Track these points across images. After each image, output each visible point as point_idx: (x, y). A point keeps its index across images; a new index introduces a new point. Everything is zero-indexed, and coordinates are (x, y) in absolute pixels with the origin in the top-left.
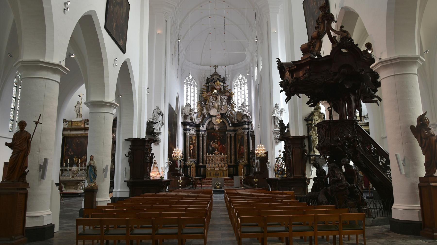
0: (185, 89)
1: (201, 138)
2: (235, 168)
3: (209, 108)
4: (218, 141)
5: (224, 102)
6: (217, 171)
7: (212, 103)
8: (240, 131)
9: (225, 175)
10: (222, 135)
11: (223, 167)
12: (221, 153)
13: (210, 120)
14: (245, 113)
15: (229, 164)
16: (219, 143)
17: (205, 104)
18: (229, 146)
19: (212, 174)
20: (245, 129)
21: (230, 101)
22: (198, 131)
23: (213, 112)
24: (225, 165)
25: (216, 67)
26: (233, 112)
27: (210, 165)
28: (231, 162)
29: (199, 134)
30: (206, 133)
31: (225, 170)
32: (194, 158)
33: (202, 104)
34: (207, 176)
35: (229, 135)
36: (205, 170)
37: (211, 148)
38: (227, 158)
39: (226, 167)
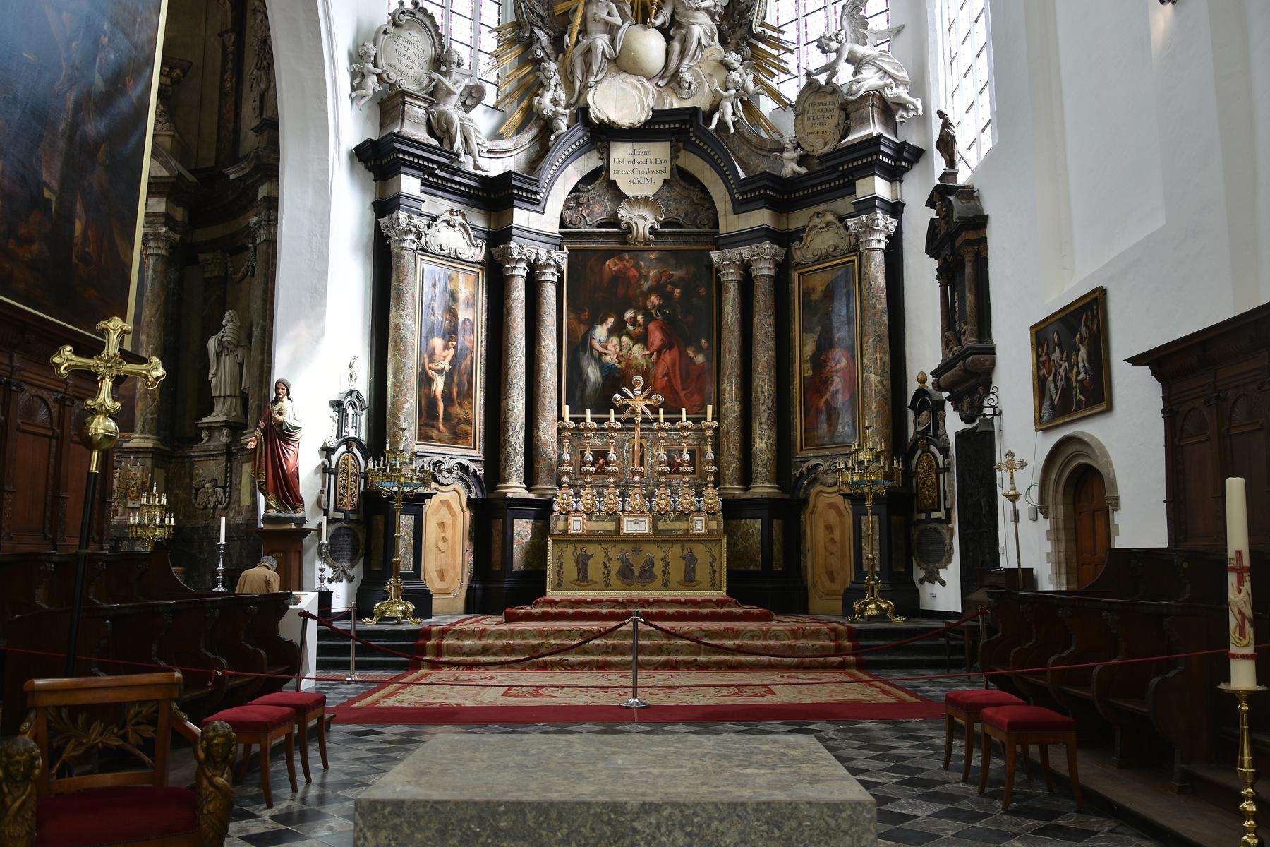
1: (518, 292)
2: (776, 525)
3: (587, 70)
4: (649, 318)
7: (611, 30)
8: (822, 241)
9: (702, 572)
10: (677, 274)
11: (684, 516)
12: (672, 410)
13: (589, 162)
14: (871, 79)
15: (735, 490)
16: (656, 337)
17: (558, 44)
18: (731, 357)
19: (595, 570)
20: (869, 205)
22: (498, 237)
23: (619, 101)
24: (699, 495)
26: (767, 106)
27: (587, 493)
28: (746, 477)
29: (507, 256)
30: (562, 258)
31: (699, 540)
32: (458, 436)
33: (532, 40)
34: (559, 585)
35: (731, 276)
36: (542, 531)
37: (593, 373)
38: (717, 448)
39: (711, 515)
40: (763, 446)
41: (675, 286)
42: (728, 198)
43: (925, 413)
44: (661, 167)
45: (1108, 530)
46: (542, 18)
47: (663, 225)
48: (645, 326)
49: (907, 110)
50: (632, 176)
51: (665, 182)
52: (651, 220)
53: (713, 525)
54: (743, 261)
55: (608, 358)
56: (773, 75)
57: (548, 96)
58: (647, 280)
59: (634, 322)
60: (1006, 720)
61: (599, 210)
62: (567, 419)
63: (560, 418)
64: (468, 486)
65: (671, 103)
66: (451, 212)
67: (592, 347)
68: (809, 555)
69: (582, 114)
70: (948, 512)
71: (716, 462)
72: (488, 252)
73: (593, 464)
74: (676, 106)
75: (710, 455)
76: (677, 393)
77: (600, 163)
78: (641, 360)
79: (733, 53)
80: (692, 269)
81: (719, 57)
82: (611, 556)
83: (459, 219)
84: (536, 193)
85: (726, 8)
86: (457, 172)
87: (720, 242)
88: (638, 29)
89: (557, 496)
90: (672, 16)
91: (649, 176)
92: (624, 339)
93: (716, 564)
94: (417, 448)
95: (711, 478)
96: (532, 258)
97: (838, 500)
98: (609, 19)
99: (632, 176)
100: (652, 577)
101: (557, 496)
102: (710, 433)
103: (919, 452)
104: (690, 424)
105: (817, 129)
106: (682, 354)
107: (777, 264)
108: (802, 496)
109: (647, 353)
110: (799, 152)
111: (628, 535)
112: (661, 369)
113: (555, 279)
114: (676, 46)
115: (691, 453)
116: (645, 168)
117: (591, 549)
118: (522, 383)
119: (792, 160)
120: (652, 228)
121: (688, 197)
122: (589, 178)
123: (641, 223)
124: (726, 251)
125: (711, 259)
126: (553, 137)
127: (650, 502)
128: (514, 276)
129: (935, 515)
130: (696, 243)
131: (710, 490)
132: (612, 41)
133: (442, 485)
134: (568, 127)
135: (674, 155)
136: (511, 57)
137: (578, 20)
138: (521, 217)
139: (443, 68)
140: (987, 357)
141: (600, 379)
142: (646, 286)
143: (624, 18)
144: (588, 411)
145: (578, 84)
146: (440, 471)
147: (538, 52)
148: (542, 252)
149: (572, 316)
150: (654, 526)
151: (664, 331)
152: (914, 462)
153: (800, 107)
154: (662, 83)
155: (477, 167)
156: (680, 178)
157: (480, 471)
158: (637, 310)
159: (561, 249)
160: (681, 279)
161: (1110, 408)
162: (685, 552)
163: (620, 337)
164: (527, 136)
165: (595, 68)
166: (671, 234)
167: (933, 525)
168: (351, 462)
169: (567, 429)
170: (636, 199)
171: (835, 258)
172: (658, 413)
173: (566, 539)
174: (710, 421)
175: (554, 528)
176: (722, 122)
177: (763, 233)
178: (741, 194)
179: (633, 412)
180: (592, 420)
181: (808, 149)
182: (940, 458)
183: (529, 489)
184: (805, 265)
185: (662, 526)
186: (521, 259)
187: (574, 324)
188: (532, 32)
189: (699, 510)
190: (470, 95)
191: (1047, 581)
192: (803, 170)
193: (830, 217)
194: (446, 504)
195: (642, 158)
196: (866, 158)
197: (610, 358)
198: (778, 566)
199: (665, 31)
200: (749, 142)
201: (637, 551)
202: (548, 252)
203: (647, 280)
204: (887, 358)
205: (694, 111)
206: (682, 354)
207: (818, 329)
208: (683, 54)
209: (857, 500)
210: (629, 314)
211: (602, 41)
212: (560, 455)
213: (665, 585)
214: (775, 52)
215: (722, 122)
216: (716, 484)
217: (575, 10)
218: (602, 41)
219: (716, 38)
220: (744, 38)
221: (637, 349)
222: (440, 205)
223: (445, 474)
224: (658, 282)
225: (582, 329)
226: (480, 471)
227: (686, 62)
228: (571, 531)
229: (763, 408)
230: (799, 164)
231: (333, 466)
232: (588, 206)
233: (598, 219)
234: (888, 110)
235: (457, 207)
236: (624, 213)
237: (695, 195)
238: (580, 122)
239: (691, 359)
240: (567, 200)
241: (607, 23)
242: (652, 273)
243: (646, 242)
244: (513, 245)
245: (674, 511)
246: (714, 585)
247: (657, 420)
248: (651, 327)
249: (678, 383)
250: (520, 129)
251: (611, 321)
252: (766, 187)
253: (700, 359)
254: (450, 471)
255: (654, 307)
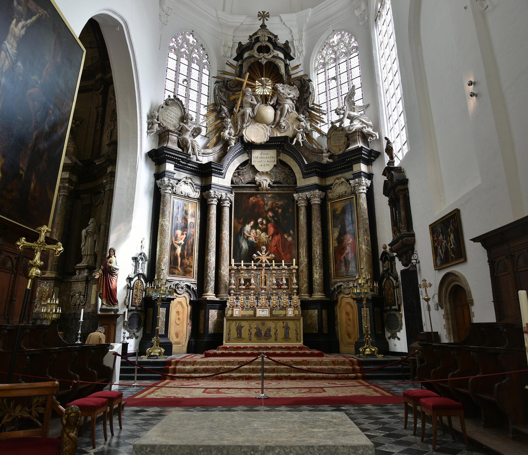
0: (172, 64)
1: (213, 211)
3: (243, 122)
4: (268, 221)
5: (288, 105)
6: (263, 319)
7: (253, 106)
8: (340, 189)
9: (292, 334)
10: (280, 203)
11: (284, 308)
12: (278, 261)
13: (244, 158)
15: (306, 296)
16: (271, 230)
17: (231, 112)
18: (303, 238)
19: (245, 333)
21: (304, 103)
22: (205, 188)
23: (255, 134)
24: (290, 298)
25: (264, 16)
26: (316, 135)
29: (209, 196)
30: (232, 197)
32: (186, 273)
35: (302, 204)
36: (222, 315)
37: (244, 245)
38: (298, 278)
39: (296, 307)
40: (318, 277)
41: (279, 208)
42: (300, 172)
43: (387, 262)
44: (273, 160)
45: (469, 315)
46: (225, 102)
47: (273, 184)
48: (267, 225)
49: (372, 137)
50: (261, 163)
51: (275, 166)
52: (269, 181)
53: (297, 312)
54: (307, 198)
55: (251, 239)
56: (318, 123)
57: (227, 132)
58: (267, 206)
59: (262, 223)
60: (431, 404)
61: (247, 177)
62: (233, 265)
63: (230, 265)
64: (190, 295)
65: (277, 134)
66: (186, 178)
67: (244, 234)
68: (339, 326)
69: (240, 139)
70: (399, 306)
71: (297, 284)
72: (201, 194)
73: (244, 285)
74: (279, 135)
75: (295, 281)
76: (280, 254)
77: (248, 158)
78: (265, 239)
79: (302, 115)
80: (286, 201)
81: (296, 116)
82: (252, 326)
83: (190, 181)
84: (222, 170)
85: (298, 98)
86: (190, 162)
87: (297, 190)
88: (263, 106)
89: (228, 299)
90: (277, 101)
91: (268, 163)
92: (258, 230)
93: (298, 330)
94: (168, 278)
95: (295, 291)
96: (219, 197)
97: (351, 301)
98: (252, 102)
99: (261, 163)
100: (270, 336)
101: (228, 299)
102: (294, 271)
103: (385, 279)
104: (286, 267)
105: (336, 144)
106: (282, 237)
107: (321, 199)
108: (335, 299)
109: (267, 236)
110: (329, 153)
111: (259, 317)
112: (273, 243)
113: (229, 205)
114: (279, 112)
115: (287, 280)
116: (266, 160)
117: (243, 323)
118: (214, 249)
119: (326, 157)
120: (269, 184)
121: (284, 172)
122: (243, 164)
123: (265, 182)
124: (300, 194)
125: (294, 197)
126: (229, 148)
127: (269, 302)
128: (212, 204)
129: (394, 307)
130: (288, 190)
131: (295, 296)
132: (253, 110)
133: (179, 294)
134: (235, 144)
135: (278, 155)
136: (212, 117)
137: (239, 103)
138: (215, 180)
139: (185, 121)
140: (412, 238)
141: (247, 248)
142: (267, 208)
143: (258, 102)
144: (242, 261)
145: (239, 127)
146: (178, 288)
147: (223, 115)
148: (224, 194)
149: (236, 221)
150: (271, 313)
151: (274, 227)
152: (383, 284)
153: (329, 136)
154: (273, 127)
155: (197, 160)
156: (281, 164)
157: (195, 288)
158: (263, 218)
159: (232, 193)
160: (282, 205)
161: (465, 260)
162: (284, 325)
163: (256, 230)
164: (218, 148)
165: (246, 121)
166: (277, 187)
167: (393, 312)
168: (140, 284)
169: (233, 269)
170: (263, 172)
171: (345, 196)
172: (272, 262)
173: (232, 319)
174: (294, 266)
175: (227, 314)
176: (297, 142)
177: (315, 186)
178: (306, 170)
179: (262, 262)
180: (244, 265)
181: (333, 152)
182: (395, 282)
183: (217, 296)
184: (333, 199)
185: (274, 313)
186: (215, 197)
187: (237, 224)
188: (221, 107)
189: (290, 306)
190: (195, 131)
191: (445, 339)
192: (331, 161)
193: (343, 180)
194: (180, 303)
195: (265, 156)
196: (357, 156)
197: (252, 239)
198: (325, 331)
199: (274, 106)
200: (308, 149)
201: (263, 324)
202: (226, 194)
203: (267, 206)
204: (369, 238)
205: (286, 137)
206: (282, 237)
207: (340, 226)
208: (281, 115)
209: (359, 301)
210: (260, 220)
211: (249, 111)
212: (230, 281)
213: (276, 340)
214: (318, 115)
215: (297, 142)
216: (298, 294)
217: (238, 99)
218: (249, 111)
219: (294, 109)
220: (306, 109)
221: (263, 235)
222: (182, 175)
223: (180, 289)
224: (272, 206)
225: (240, 226)
226: (195, 288)
227: (283, 118)
228: (235, 315)
229: (317, 260)
230: (329, 158)
231: (132, 286)
232: (243, 175)
233: (247, 181)
234: (365, 137)
235: (189, 176)
236: (258, 178)
237: (287, 171)
238: (240, 142)
239: (286, 239)
240: (234, 173)
241: (251, 104)
242: (269, 203)
243: (267, 190)
244: (211, 191)
245: (279, 306)
246: (298, 340)
247: (272, 265)
248: (269, 225)
249: (280, 249)
250: (215, 145)
251: (252, 223)
252: (316, 168)
253: (290, 239)
254: (182, 288)
255: (270, 217)
